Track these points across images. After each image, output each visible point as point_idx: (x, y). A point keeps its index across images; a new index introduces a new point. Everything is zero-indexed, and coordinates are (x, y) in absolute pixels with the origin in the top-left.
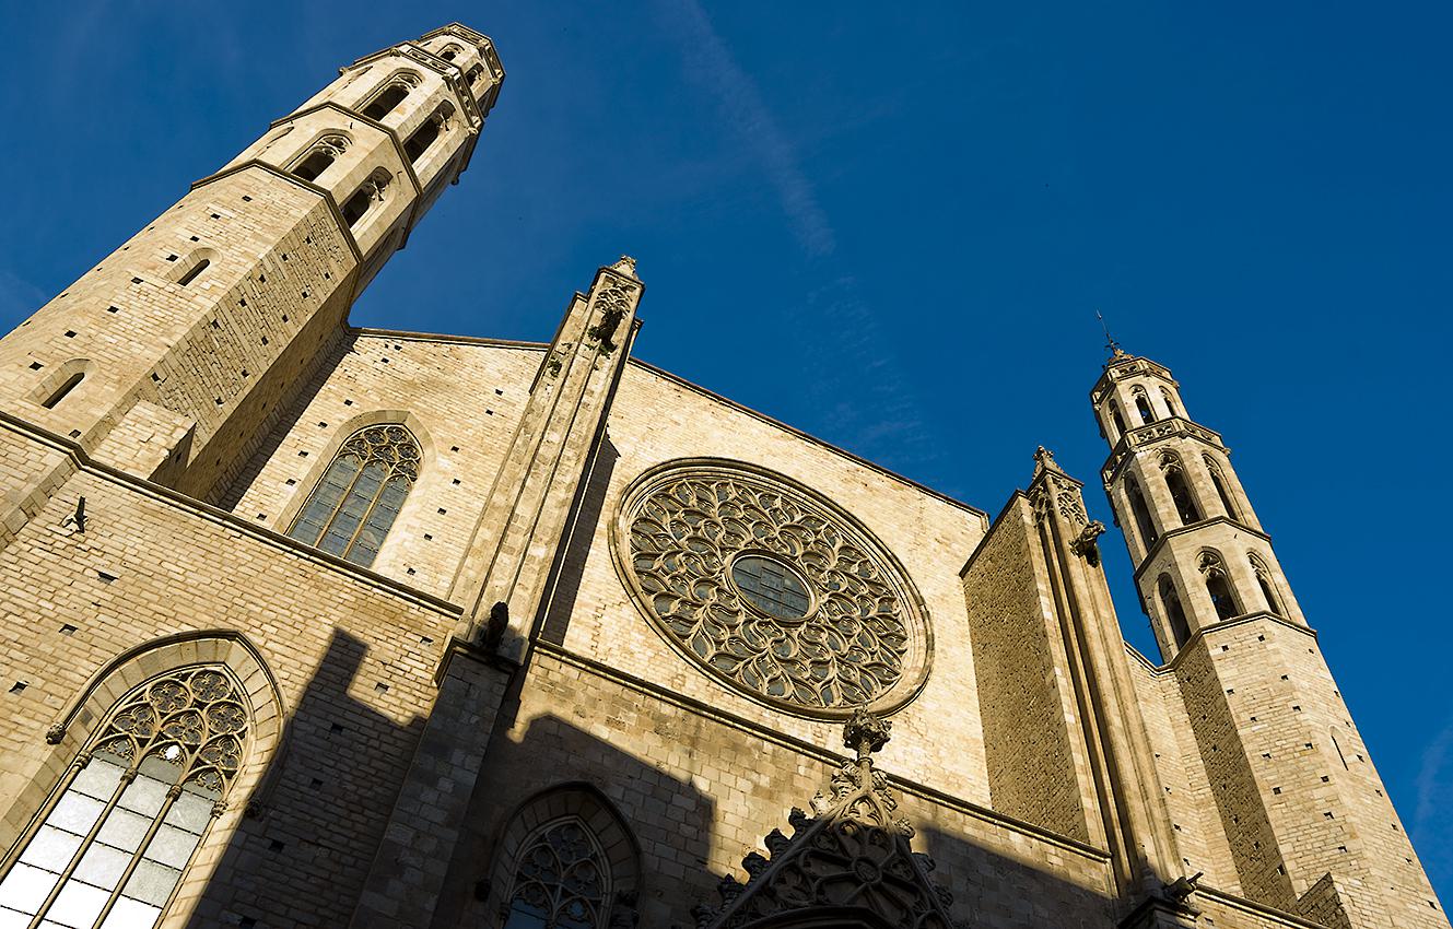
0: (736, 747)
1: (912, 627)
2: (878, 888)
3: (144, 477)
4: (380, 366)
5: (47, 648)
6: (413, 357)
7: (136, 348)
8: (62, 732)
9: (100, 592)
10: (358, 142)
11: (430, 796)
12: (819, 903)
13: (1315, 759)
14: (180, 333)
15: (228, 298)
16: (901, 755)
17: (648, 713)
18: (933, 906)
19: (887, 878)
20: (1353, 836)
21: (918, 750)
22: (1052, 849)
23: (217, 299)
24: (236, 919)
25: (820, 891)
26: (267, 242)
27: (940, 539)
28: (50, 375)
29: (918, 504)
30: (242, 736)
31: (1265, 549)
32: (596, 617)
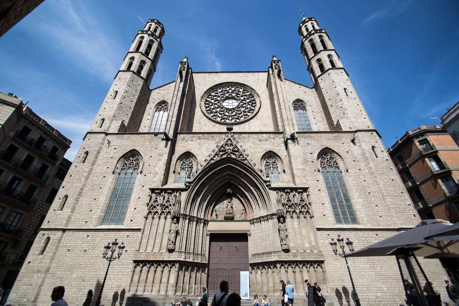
0: (212, 137)
1: (257, 100)
2: (231, 153)
3: (117, 132)
4: (157, 94)
5: (110, 161)
6: (162, 90)
7: (110, 113)
8: (114, 171)
9: (115, 151)
10: (136, 57)
11: (161, 162)
13: (339, 97)
14: (116, 107)
15: (122, 98)
18: (241, 152)
19: (233, 151)
20: (346, 110)
21: (258, 122)
23: (120, 99)
24: (142, 186)
25: (221, 156)
26: (125, 85)
28: (99, 122)
29: (258, 75)
30: (139, 162)
31: (333, 53)
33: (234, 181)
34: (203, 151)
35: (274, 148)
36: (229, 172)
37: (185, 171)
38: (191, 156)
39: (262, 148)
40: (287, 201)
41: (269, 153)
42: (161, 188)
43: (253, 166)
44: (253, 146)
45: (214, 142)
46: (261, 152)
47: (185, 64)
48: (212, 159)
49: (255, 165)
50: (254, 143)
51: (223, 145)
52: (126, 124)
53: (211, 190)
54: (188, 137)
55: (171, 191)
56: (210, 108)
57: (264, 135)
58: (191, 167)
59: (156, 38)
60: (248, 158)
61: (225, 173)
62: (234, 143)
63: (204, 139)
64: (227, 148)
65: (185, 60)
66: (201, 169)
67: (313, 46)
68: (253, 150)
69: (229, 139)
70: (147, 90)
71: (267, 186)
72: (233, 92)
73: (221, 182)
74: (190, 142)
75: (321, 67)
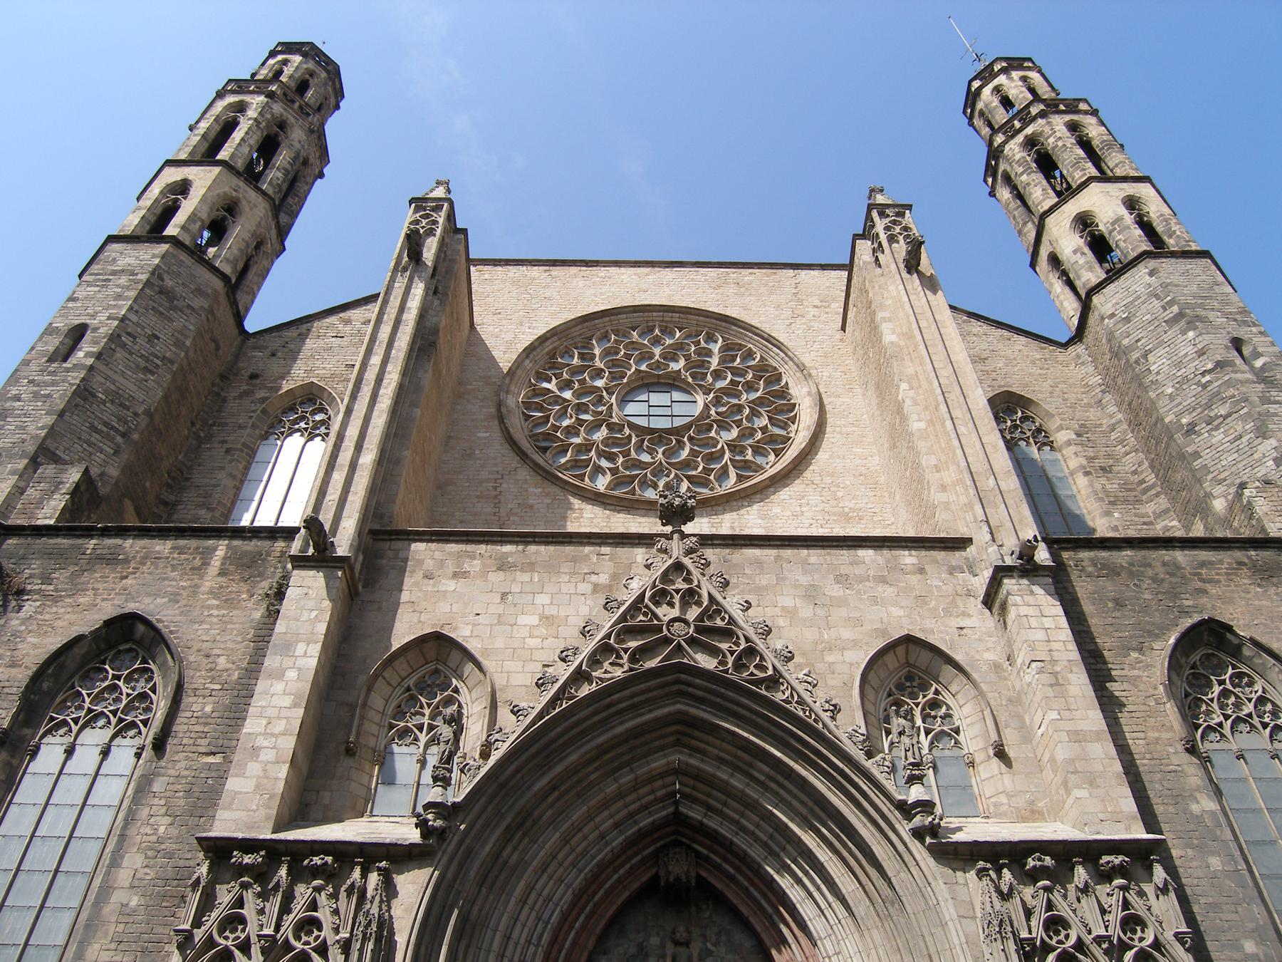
1: (800, 393)
11: (279, 687)
12: (631, 670)
16: (798, 509)
17: (491, 557)
18: (747, 640)
19: (698, 630)
21: (814, 498)
22: (907, 553)
25: (633, 659)
27: (819, 304)
32: (495, 488)
33: (710, 808)
34: (524, 632)
35: (929, 624)
36: (676, 757)
37: (413, 749)
38: (452, 664)
39: (859, 622)
40: (1047, 929)
41: (900, 650)
42: (269, 836)
43: (826, 716)
44: (806, 611)
45: (585, 588)
46: (856, 644)
47: (438, 209)
48: (579, 676)
49: (835, 710)
50: (812, 594)
51: (642, 595)
52: (104, 490)
53: (574, 864)
54: (438, 555)
55: (329, 859)
56: (556, 428)
57: (866, 554)
58: (456, 721)
59: (303, 112)
60: (793, 674)
61: (658, 763)
62: (707, 588)
63: (531, 567)
64: (666, 613)
65: (440, 193)
66: (512, 729)
67: (1046, 164)
68: (810, 634)
69: (678, 567)
70: (234, 331)
71: (918, 834)
72: (670, 356)
73: (631, 815)
74: (450, 585)
75: (1100, 246)
